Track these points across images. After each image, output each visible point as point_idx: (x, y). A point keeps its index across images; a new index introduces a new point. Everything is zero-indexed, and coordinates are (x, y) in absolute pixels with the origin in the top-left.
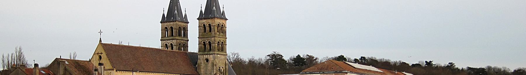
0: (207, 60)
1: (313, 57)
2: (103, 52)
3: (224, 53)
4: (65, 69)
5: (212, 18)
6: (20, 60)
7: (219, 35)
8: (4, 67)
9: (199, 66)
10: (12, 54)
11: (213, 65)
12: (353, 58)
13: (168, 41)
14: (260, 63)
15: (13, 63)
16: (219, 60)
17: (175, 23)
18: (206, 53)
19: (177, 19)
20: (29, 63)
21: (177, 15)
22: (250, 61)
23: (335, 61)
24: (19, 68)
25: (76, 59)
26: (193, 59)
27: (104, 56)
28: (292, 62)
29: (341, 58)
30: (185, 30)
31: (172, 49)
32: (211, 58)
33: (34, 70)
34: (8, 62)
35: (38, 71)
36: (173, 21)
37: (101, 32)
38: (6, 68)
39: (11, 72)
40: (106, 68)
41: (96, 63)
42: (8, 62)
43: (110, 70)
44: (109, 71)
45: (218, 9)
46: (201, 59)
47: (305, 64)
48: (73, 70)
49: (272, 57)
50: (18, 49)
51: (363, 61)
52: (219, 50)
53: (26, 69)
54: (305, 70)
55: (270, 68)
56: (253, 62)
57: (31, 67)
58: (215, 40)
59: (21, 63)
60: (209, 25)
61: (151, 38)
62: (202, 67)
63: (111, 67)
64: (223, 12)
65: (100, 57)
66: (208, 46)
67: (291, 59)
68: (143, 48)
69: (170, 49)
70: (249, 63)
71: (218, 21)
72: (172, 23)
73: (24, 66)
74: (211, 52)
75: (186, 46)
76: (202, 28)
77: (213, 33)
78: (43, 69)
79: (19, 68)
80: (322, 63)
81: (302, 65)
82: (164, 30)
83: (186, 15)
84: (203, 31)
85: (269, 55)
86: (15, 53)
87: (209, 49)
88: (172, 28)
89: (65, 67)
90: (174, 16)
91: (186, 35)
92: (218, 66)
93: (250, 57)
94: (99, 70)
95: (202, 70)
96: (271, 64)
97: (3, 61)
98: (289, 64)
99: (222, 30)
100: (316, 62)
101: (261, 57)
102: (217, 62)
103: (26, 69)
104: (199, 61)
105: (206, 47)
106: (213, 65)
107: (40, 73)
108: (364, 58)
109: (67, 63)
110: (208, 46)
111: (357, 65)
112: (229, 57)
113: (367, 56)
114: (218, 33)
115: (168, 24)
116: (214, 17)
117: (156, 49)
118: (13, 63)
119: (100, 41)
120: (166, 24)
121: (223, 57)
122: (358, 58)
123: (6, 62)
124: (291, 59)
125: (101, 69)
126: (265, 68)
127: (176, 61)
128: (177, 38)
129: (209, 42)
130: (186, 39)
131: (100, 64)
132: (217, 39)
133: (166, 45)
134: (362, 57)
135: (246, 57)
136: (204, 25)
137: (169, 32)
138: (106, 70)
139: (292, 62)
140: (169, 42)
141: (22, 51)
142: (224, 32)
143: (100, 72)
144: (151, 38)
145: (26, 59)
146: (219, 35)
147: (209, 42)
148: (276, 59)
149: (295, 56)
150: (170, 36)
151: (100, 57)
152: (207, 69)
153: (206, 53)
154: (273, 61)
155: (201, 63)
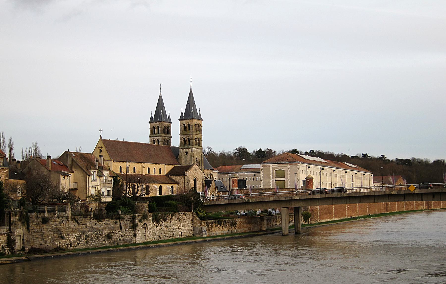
0: (187, 153)
1: (272, 151)
2: (103, 146)
3: (201, 147)
4: (73, 160)
5: (190, 119)
6: (36, 153)
7: (196, 133)
8: (23, 158)
9: (180, 157)
10: (30, 148)
11: (191, 157)
12: (304, 152)
13: (155, 138)
14: (229, 155)
15: (30, 155)
16: (196, 153)
17: (160, 123)
18: (186, 147)
19: (163, 120)
20: (43, 155)
21: (162, 117)
22: (221, 154)
23: (289, 154)
24: (36, 159)
25: (81, 152)
26: (175, 151)
27: (104, 149)
28: (255, 154)
29: (295, 151)
30: (169, 128)
31: (159, 144)
32: (189, 151)
33: (47, 161)
34: (27, 154)
35: (50, 161)
36: (159, 120)
37: (101, 130)
38: (25, 160)
39: (29, 163)
40: (105, 159)
41: (97, 155)
42: (27, 154)
43: (108, 161)
44: (108, 162)
45: (195, 112)
46: (182, 152)
47: (265, 156)
48: (78, 161)
49: (239, 151)
50: (35, 144)
51: (312, 153)
52: (196, 145)
53: (41, 160)
54: (266, 161)
55: (237, 159)
56: (224, 154)
57: (45, 158)
58: (193, 137)
59: (37, 155)
60: (189, 124)
61: (141, 134)
62: (182, 158)
63: (109, 159)
64: (200, 114)
65: (101, 151)
66: (187, 142)
67: (254, 152)
68: (135, 143)
69: (156, 144)
70: (220, 155)
71: (195, 122)
72: (158, 123)
73: (39, 157)
74: (190, 147)
75: (169, 142)
76: (183, 127)
77: (191, 131)
78: (55, 160)
79: (36, 159)
80: (279, 155)
81: (263, 157)
82: (152, 128)
83: (169, 117)
84: (183, 129)
85: (236, 149)
86: (32, 147)
87: (188, 144)
88: (158, 127)
89: (72, 159)
90: (160, 117)
91: (169, 133)
92: (195, 158)
93: (221, 151)
94: (100, 161)
95: (183, 161)
96: (238, 156)
97: (23, 154)
98: (253, 156)
99: (199, 128)
100: (275, 155)
101: (230, 151)
102: (195, 154)
103: (41, 160)
104: (180, 154)
105: (185, 142)
106: (191, 157)
107: (52, 163)
108: (313, 151)
109: (74, 155)
110: (187, 142)
111: (307, 157)
112: (204, 150)
113: (315, 150)
114: (195, 131)
115: (155, 123)
116: (193, 118)
117: (145, 144)
118: (30, 155)
119: (101, 137)
120: (153, 124)
121: (199, 150)
122: (308, 151)
123: (25, 154)
124: (254, 152)
125: (101, 160)
126: (233, 159)
127: (162, 153)
128: (162, 135)
129: (188, 138)
130: (170, 136)
131: (101, 156)
132: (195, 136)
133: (154, 140)
134: (311, 151)
135: (217, 150)
136: (184, 125)
137: (156, 130)
138: (105, 161)
139: (255, 154)
140: (156, 139)
141: (38, 145)
142: (200, 130)
143: (100, 163)
144: (141, 134)
145: (41, 152)
146: (196, 133)
147: (188, 138)
148: (242, 152)
149: (258, 149)
150: (157, 134)
151: (101, 151)
152: (186, 160)
153: (186, 147)
154: (240, 154)
155: (182, 155)
